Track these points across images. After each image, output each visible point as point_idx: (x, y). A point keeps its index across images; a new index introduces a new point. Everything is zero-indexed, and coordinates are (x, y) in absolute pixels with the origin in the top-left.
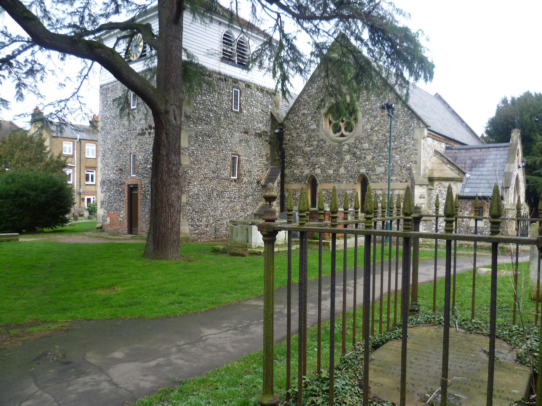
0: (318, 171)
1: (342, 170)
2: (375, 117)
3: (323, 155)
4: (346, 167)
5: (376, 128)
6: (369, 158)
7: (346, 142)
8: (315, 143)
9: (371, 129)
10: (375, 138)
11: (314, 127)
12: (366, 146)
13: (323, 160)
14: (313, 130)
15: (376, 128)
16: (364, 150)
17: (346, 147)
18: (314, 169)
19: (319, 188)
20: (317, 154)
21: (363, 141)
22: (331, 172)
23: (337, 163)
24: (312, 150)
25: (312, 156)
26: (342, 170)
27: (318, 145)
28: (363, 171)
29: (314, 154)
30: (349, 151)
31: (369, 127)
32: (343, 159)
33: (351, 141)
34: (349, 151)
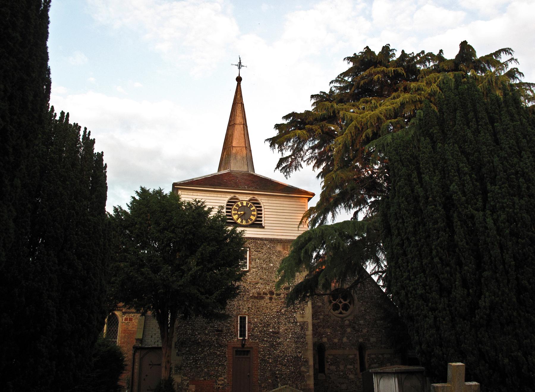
0: (325, 340)
1: (345, 340)
2: (367, 302)
3: (328, 327)
4: (348, 338)
5: (368, 311)
6: (365, 331)
7: (347, 318)
8: (321, 317)
9: (365, 310)
10: (368, 317)
11: (320, 304)
12: (362, 322)
13: (328, 331)
14: (320, 307)
15: (368, 311)
16: (360, 325)
17: (347, 322)
18: (321, 338)
19: (327, 353)
20: (324, 326)
21: (359, 319)
22: (336, 340)
23: (340, 334)
24: (318, 322)
25: (319, 327)
26: (345, 340)
27: (323, 319)
28: (361, 340)
29: (321, 326)
30: (349, 326)
31: (363, 309)
32: (345, 331)
33: (350, 318)
34: (349, 326)
